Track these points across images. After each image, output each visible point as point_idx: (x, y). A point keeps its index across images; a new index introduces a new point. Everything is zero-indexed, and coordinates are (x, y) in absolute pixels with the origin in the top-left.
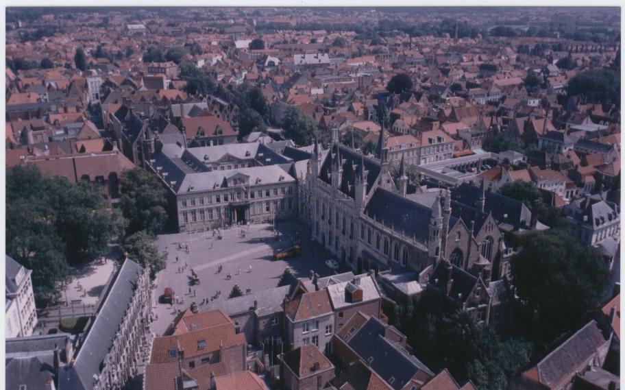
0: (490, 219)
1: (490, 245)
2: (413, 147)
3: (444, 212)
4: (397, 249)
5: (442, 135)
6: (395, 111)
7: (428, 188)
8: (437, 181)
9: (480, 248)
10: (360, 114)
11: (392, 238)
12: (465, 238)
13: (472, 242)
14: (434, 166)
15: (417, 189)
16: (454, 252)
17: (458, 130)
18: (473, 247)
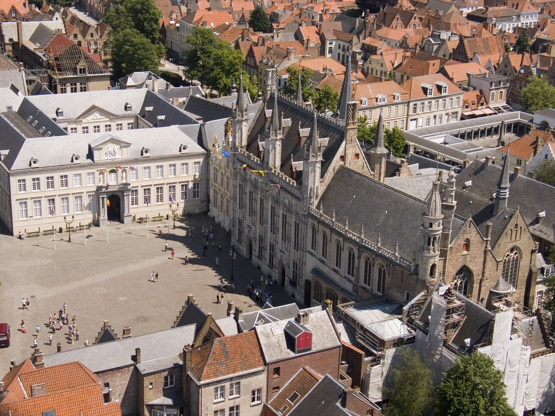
0: (518, 219)
1: (516, 262)
2: (396, 101)
3: (446, 208)
4: (368, 266)
5: (443, 82)
6: (368, 41)
7: (420, 167)
8: (433, 156)
9: (501, 266)
10: (311, 45)
11: (362, 248)
12: (477, 248)
13: (489, 256)
14: (430, 132)
15: (403, 170)
16: (459, 272)
17: (468, 75)
18: (490, 264)
